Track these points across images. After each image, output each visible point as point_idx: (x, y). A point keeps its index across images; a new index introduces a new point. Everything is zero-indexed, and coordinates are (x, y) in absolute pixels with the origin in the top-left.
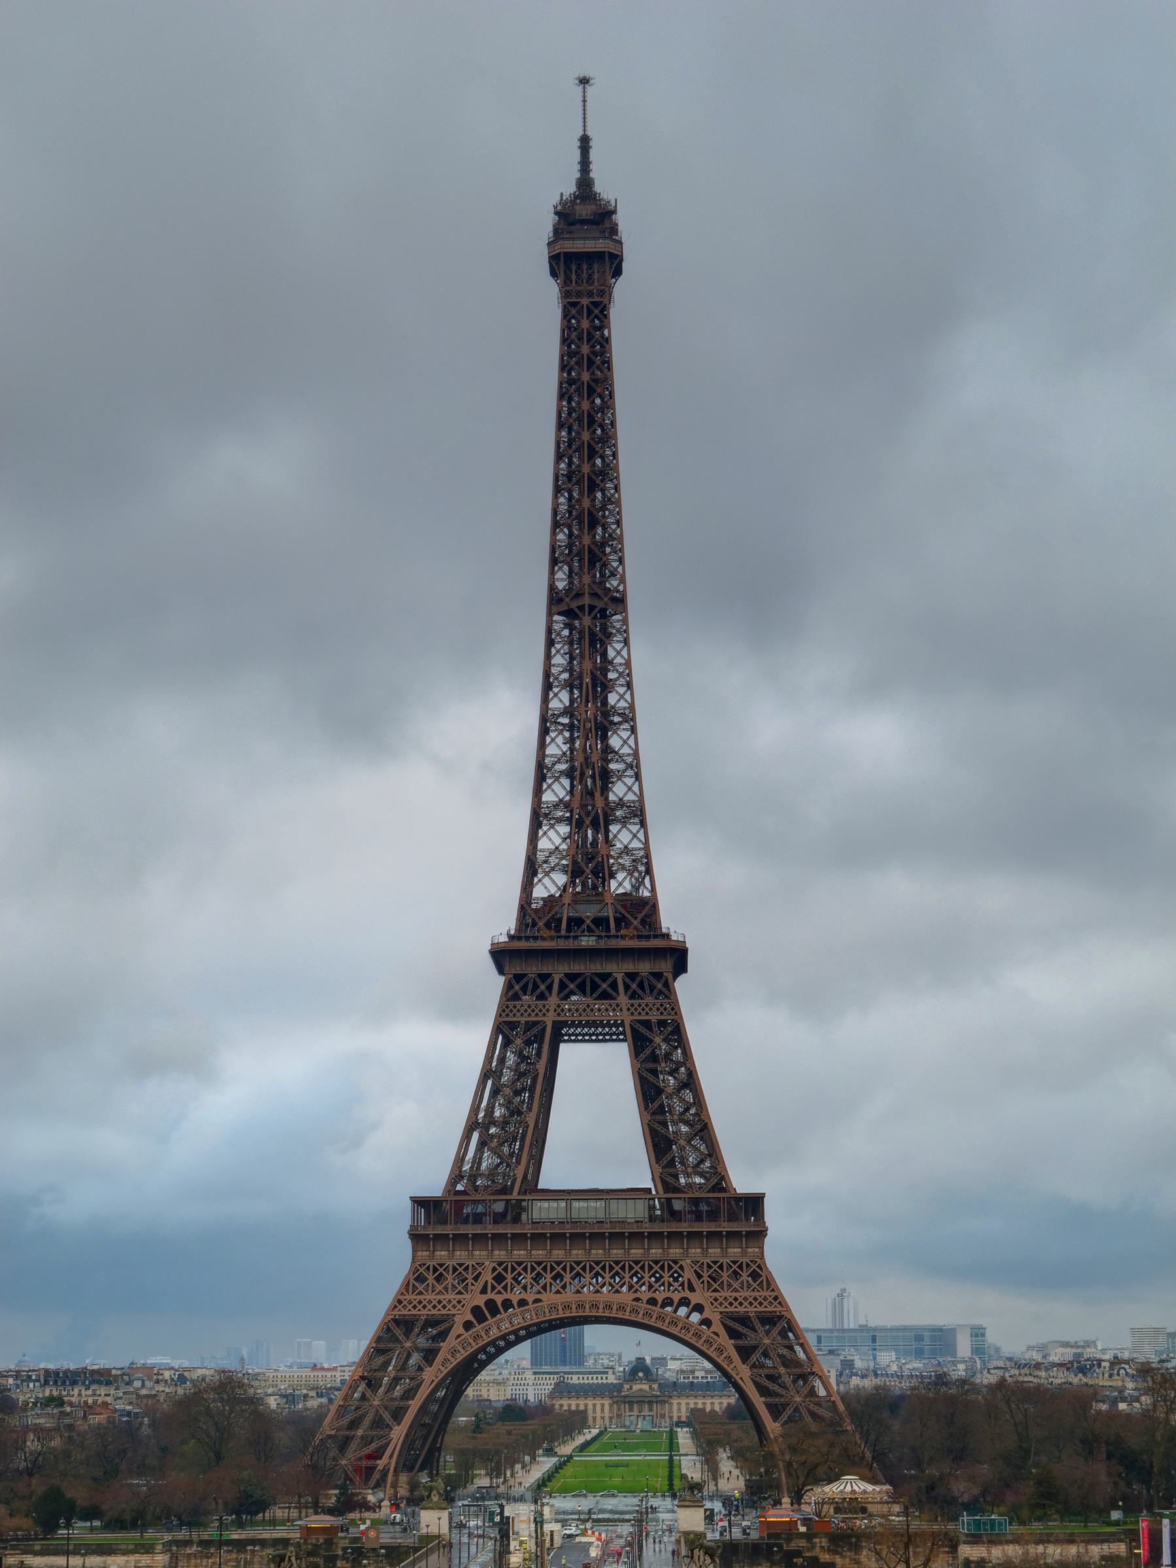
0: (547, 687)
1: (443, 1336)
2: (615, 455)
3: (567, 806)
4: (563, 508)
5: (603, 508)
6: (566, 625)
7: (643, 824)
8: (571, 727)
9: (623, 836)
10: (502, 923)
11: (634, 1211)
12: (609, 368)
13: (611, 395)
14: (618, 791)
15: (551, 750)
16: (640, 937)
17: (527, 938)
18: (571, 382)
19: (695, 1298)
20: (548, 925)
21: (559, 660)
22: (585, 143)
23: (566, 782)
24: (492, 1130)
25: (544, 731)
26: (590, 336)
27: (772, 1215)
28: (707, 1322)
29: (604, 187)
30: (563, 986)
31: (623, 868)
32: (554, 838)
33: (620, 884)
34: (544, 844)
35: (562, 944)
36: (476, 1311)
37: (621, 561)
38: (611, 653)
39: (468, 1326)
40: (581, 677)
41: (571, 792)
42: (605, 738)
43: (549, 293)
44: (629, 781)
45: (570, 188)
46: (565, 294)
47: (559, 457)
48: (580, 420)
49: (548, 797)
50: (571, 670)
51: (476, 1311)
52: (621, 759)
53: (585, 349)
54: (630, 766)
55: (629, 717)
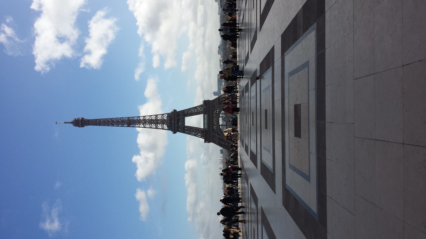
9: (159, 118)
11: (206, 116)
14: (154, 118)
15: (148, 126)
22: (65, 123)
32: (160, 126)
33: (165, 118)
34: (161, 127)
35: (173, 124)
36: (218, 134)
43: (86, 127)
45: (72, 125)
51: (218, 134)
55: (144, 117)
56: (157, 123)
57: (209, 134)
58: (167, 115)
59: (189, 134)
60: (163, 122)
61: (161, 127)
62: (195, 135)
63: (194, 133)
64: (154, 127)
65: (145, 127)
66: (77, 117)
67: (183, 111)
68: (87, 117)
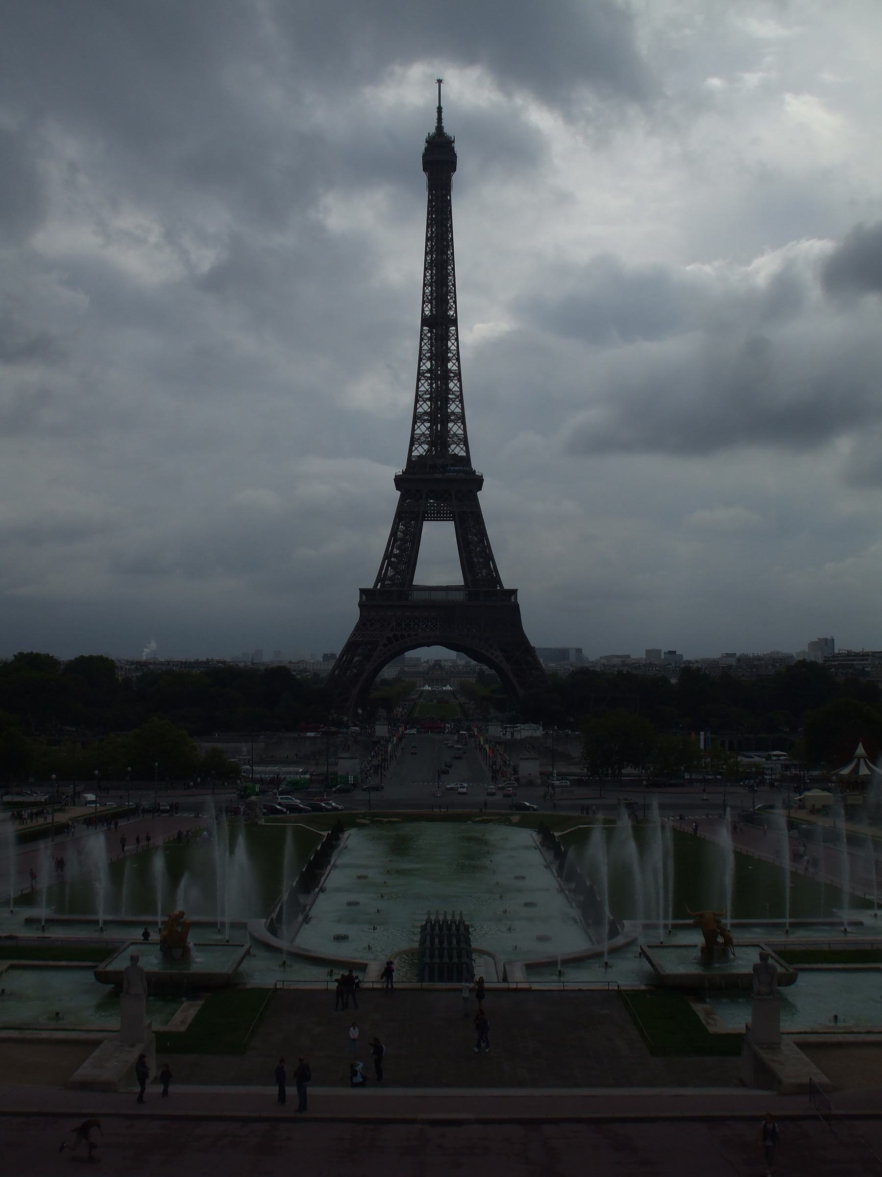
0: (420, 359)
4: (429, 278)
6: (430, 331)
7: (464, 423)
9: (454, 428)
10: (400, 468)
11: (460, 596)
14: (453, 407)
15: (422, 389)
18: (432, 219)
22: (440, 110)
23: (429, 403)
24: (393, 559)
25: (419, 380)
27: (521, 599)
29: (448, 130)
31: (455, 443)
32: (423, 428)
34: (418, 431)
37: (455, 302)
38: (450, 344)
39: (385, 645)
42: (447, 384)
44: (457, 403)
45: (433, 130)
46: (430, 179)
48: (436, 236)
49: (420, 410)
50: (431, 353)
54: (457, 397)
55: (458, 375)
56: (433, 420)
57: (392, 605)
59: (393, 534)
60: (439, 439)
62: (387, 556)
63: (396, 551)
64: (420, 410)
65: (420, 375)
66: (459, 148)
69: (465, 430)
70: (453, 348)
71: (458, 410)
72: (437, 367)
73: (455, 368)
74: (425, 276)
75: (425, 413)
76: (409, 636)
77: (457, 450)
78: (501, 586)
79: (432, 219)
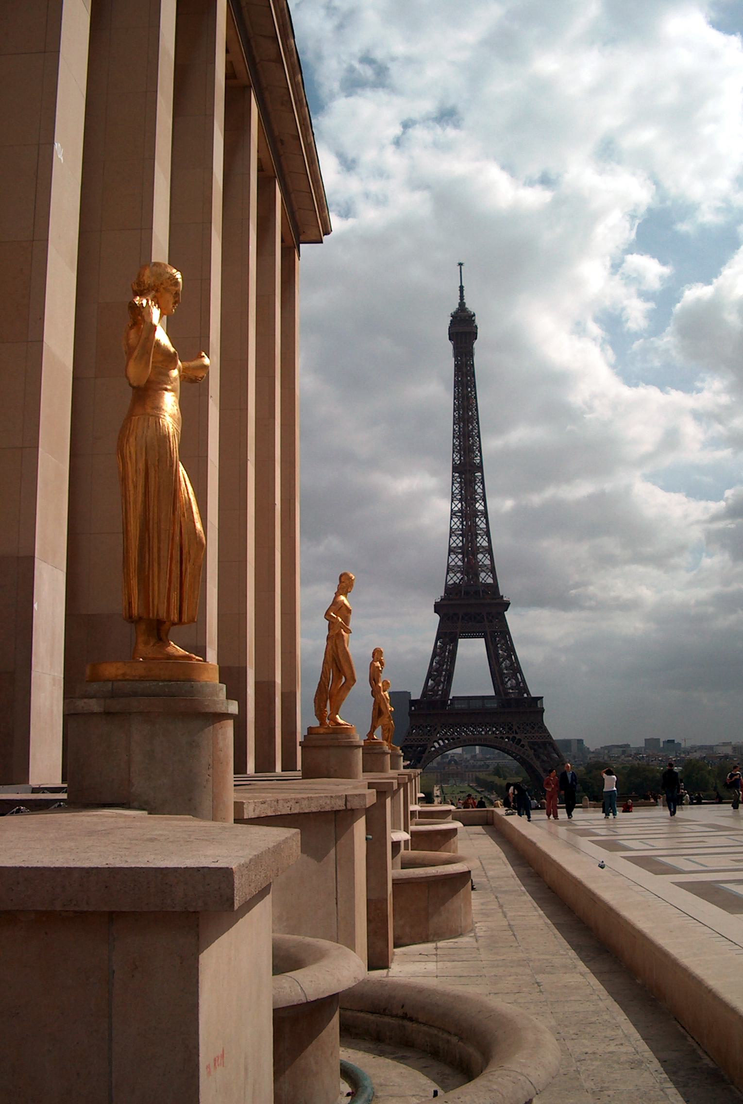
1: (423, 752)
2: (477, 410)
3: (460, 548)
5: (472, 430)
8: (461, 517)
10: (439, 593)
11: (494, 705)
12: (474, 376)
13: (475, 386)
14: (482, 542)
16: (493, 599)
17: (449, 600)
19: (518, 737)
20: (457, 594)
21: (457, 491)
22: (461, 288)
23: (461, 538)
26: (466, 364)
28: (523, 746)
29: (470, 306)
30: (463, 618)
32: (457, 560)
37: (480, 451)
40: (466, 498)
41: (462, 541)
47: (454, 411)
52: (481, 529)
53: (465, 370)
55: (485, 514)
58: (490, 581)
60: (470, 568)
61: (453, 563)
64: (454, 545)
65: (453, 513)
66: (478, 321)
67: (505, 632)
68: (478, 346)
69: (492, 560)
70: (479, 491)
71: (485, 544)
72: (466, 508)
73: (481, 508)
74: (454, 430)
75: (457, 547)
76: (453, 739)
77: (485, 578)
78: (528, 694)
79: (459, 381)
